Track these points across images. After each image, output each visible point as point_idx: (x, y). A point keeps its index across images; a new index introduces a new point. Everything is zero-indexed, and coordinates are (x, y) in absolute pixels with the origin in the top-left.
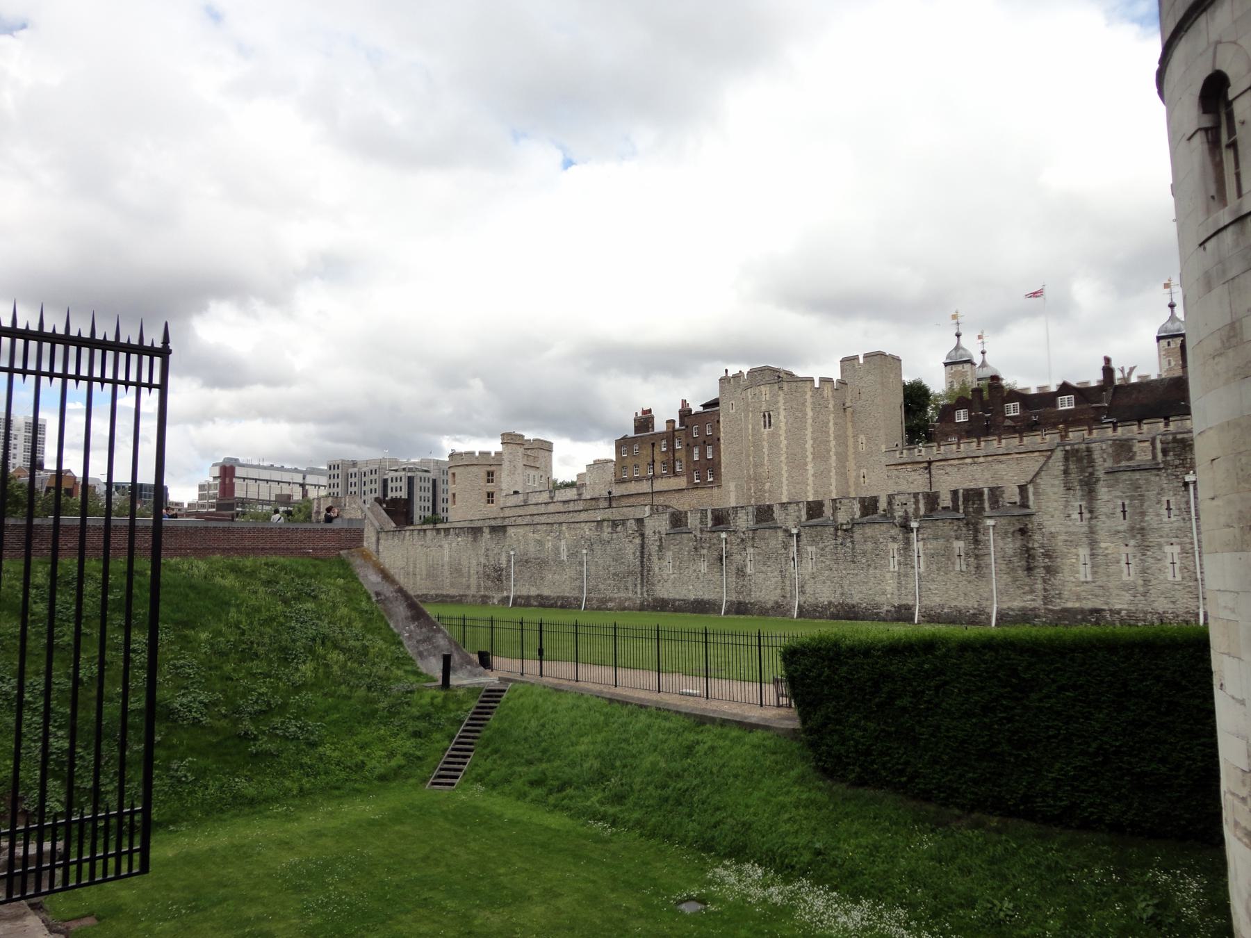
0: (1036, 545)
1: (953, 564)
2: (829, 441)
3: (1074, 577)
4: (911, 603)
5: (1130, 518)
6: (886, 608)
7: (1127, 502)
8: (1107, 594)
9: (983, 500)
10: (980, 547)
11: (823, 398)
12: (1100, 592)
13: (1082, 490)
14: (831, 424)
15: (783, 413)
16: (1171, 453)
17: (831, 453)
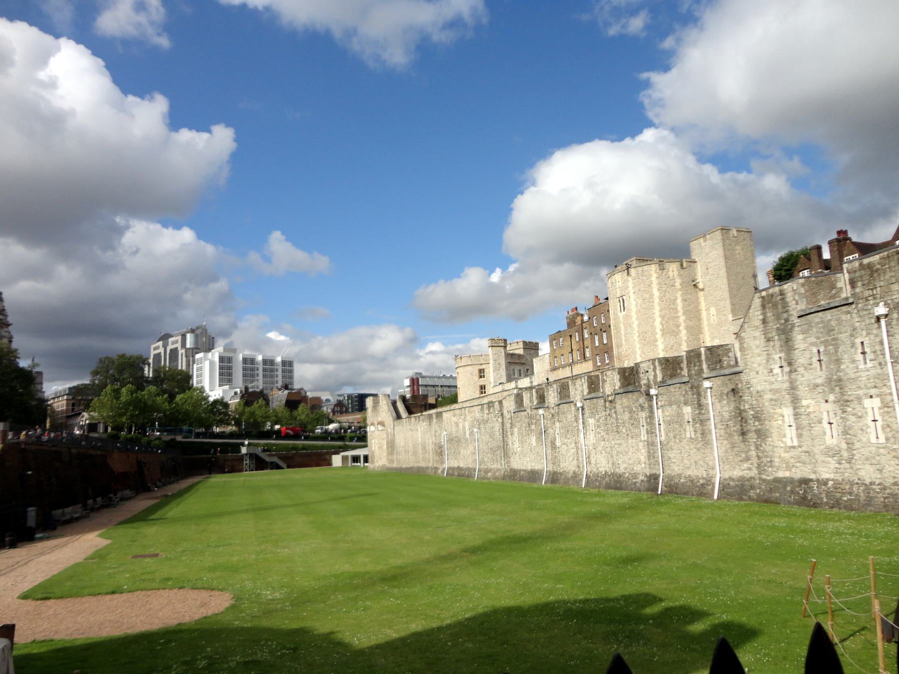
0: (747, 407)
1: (685, 430)
2: (678, 317)
3: (782, 441)
4: (658, 473)
5: (827, 368)
6: (641, 478)
7: (822, 349)
8: (814, 461)
9: (702, 361)
10: (703, 411)
11: (669, 277)
12: (804, 457)
13: (780, 340)
14: (679, 301)
15: (633, 296)
16: (859, 284)
17: (682, 328)
